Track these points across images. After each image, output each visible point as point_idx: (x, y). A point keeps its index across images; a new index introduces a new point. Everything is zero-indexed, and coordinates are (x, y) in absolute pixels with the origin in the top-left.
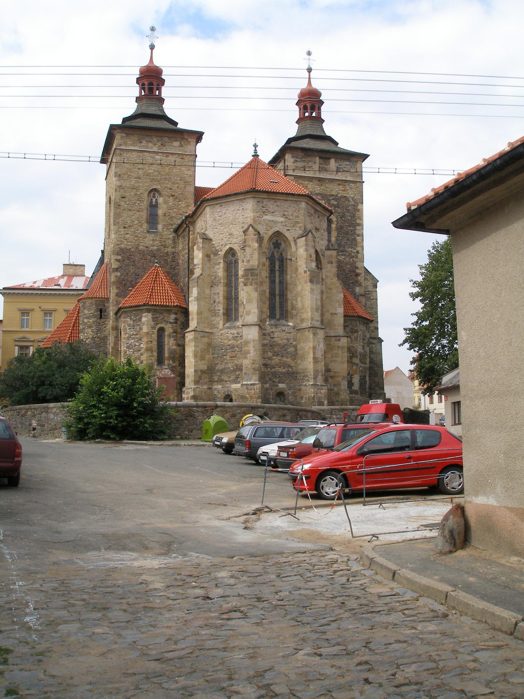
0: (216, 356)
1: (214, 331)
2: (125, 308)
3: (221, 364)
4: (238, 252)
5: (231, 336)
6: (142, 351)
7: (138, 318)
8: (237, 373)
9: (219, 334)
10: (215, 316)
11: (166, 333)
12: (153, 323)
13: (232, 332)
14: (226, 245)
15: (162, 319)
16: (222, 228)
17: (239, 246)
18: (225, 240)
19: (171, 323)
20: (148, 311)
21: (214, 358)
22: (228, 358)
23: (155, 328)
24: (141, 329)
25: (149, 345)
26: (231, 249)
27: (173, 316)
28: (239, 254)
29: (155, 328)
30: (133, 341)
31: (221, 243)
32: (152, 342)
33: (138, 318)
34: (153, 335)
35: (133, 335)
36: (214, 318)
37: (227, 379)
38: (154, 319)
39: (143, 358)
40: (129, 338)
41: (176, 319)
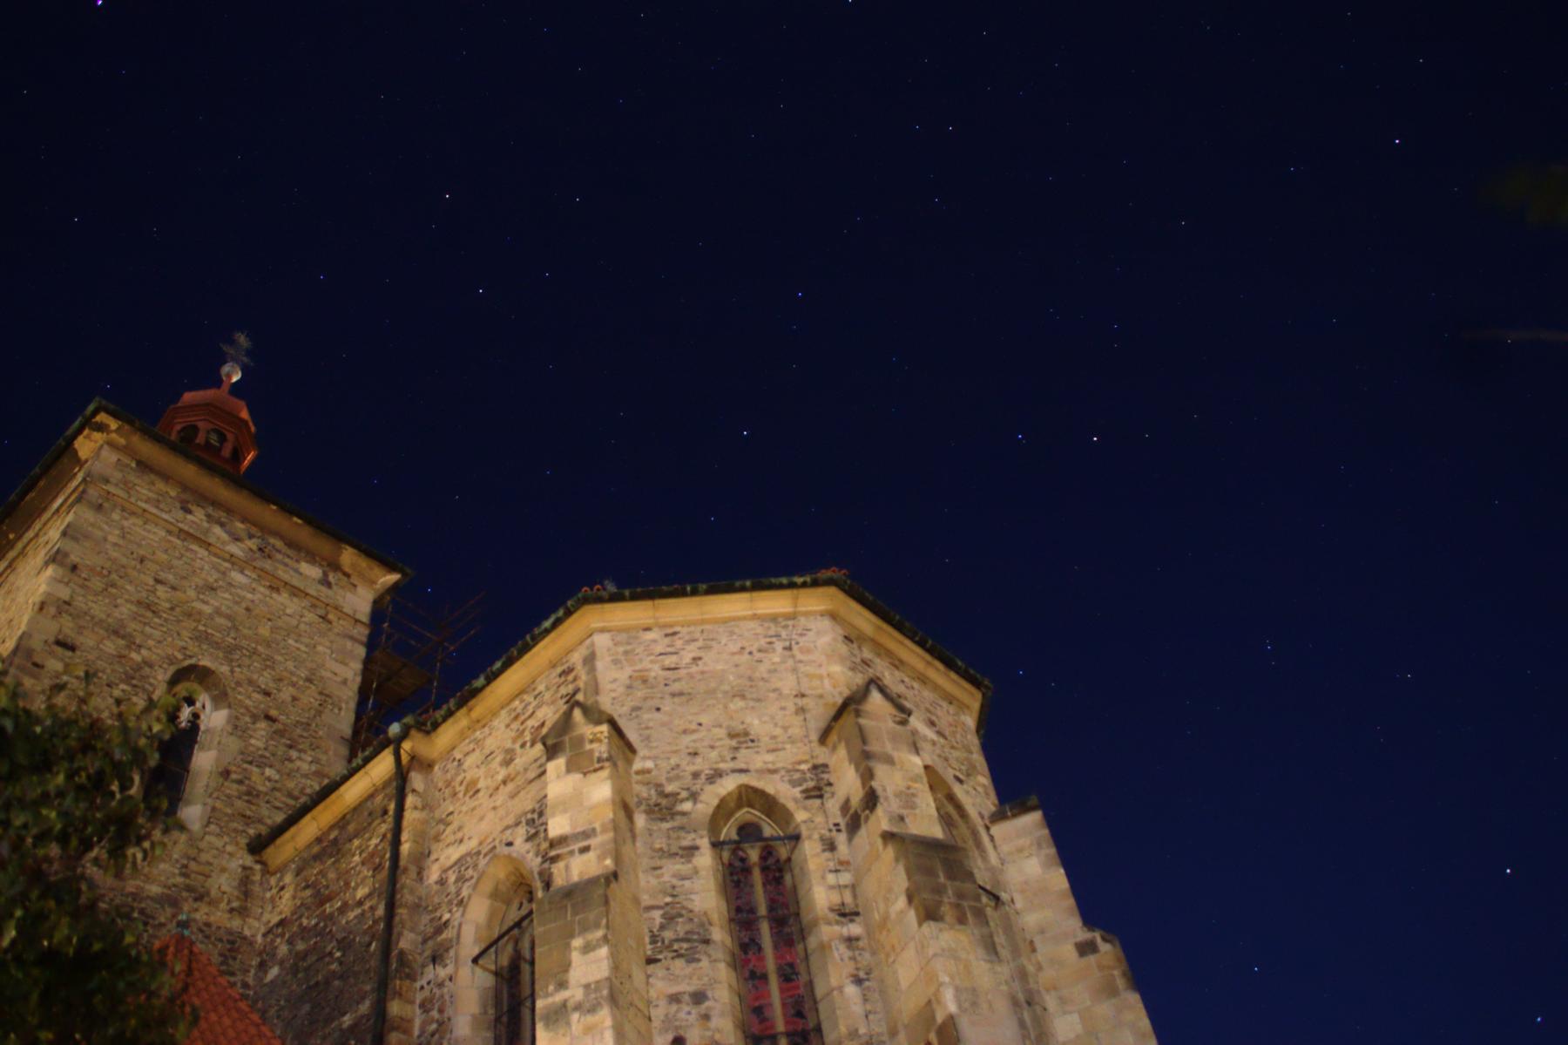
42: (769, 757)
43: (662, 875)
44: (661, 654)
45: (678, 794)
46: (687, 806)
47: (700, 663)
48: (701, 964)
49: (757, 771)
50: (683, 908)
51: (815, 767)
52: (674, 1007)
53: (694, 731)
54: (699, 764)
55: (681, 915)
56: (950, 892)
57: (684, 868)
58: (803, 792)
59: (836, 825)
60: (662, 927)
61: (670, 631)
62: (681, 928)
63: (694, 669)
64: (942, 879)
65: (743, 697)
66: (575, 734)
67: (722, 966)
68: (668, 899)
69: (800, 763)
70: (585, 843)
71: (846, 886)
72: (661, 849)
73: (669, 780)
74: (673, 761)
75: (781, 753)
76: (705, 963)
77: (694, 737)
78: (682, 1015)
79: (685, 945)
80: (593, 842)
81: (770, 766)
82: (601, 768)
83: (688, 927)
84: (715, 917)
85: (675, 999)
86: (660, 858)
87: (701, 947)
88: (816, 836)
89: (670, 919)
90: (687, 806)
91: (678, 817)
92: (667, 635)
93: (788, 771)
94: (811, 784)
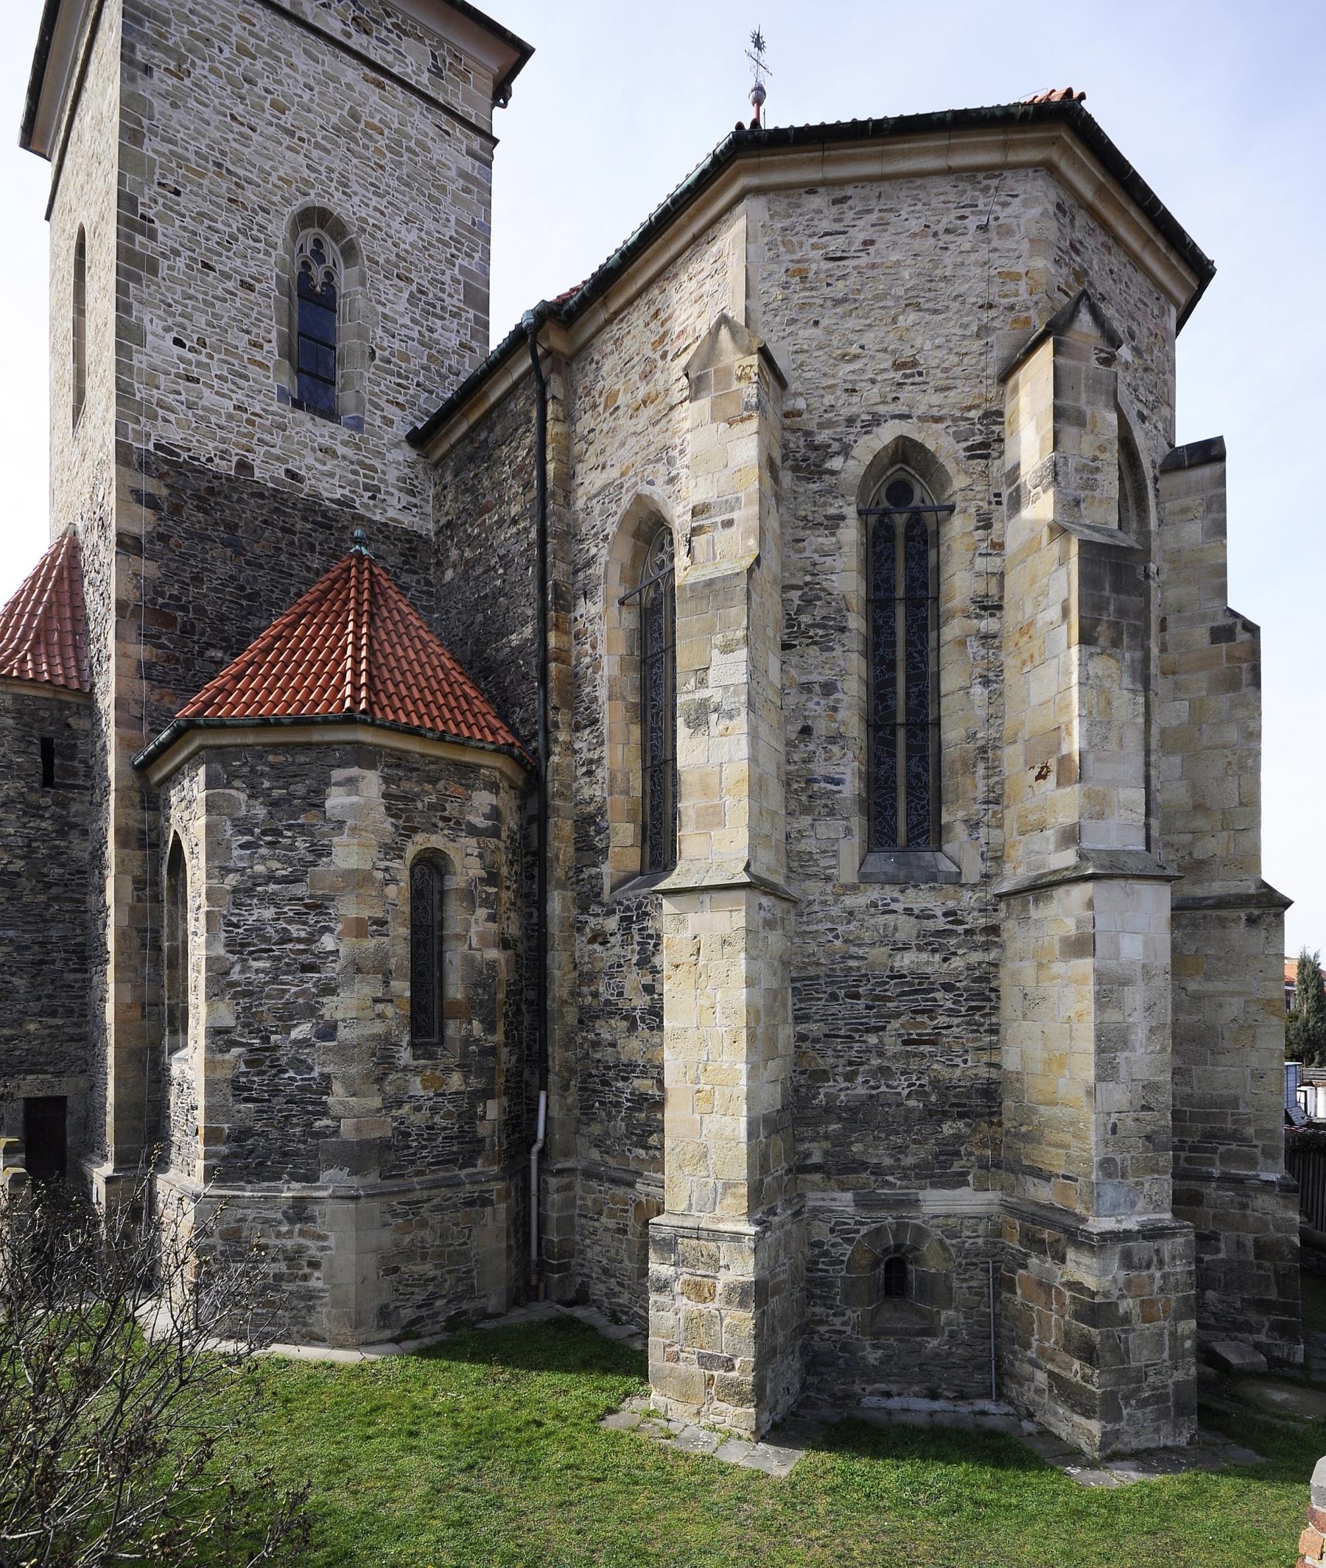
0: (814, 1028)
1: (814, 889)
2: (221, 726)
3: (850, 1077)
4: (951, 467)
5: (907, 929)
6: (331, 970)
7: (300, 789)
8: (947, 1129)
9: (835, 911)
10: (806, 810)
11: (456, 881)
12: (388, 825)
13: (917, 908)
14: (876, 420)
15: (431, 807)
16: (851, 323)
17: (959, 437)
18: (873, 394)
19: (473, 831)
20: (363, 756)
21: (802, 1038)
22: (892, 1046)
23: (398, 852)
24: (321, 852)
25: (370, 943)
26: (906, 451)
27: (483, 799)
28: (959, 482)
29: (398, 852)
30: (269, 913)
31: (846, 412)
32: (382, 923)
33: (300, 789)
34: (391, 890)
35: (271, 878)
36: (807, 820)
37: (888, 1161)
38: (396, 804)
39: (338, 1007)
40: (242, 895)
41: (495, 814)
42: (936, 399)
43: (804, 549)
44: (826, 234)
45: (829, 446)
46: (836, 463)
47: (872, 249)
48: (834, 653)
49: (919, 417)
50: (824, 590)
51: (987, 415)
52: (805, 697)
53: (856, 357)
54: (856, 406)
55: (819, 599)
56: (1112, 608)
57: (827, 542)
58: (967, 449)
59: (998, 495)
60: (799, 611)
61: (839, 193)
62: (819, 612)
63: (864, 260)
64: (1107, 593)
65: (918, 307)
66: (721, 365)
67: (854, 656)
68: (808, 578)
69: (969, 408)
70: (726, 517)
71: (994, 574)
72: (805, 518)
73: (821, 426)
74: (828, 400)
75: (952, 393)
76: (838, 651)
77: (857, 365)
78: (811, 705)
79: (821, 632)
80: (735, 515)
81: (935, 412)
82: (750, 417)
83: (824, 612)
84: (854, 601)
85: (806, 688)
86: (804, 528)
87: (836, 635)
88: (972, 510)
89: (808, 602)
90: (836, 463)
91: (827, 477)
92: (835, 202)
93: (955, 420)
94: (978, 439)
